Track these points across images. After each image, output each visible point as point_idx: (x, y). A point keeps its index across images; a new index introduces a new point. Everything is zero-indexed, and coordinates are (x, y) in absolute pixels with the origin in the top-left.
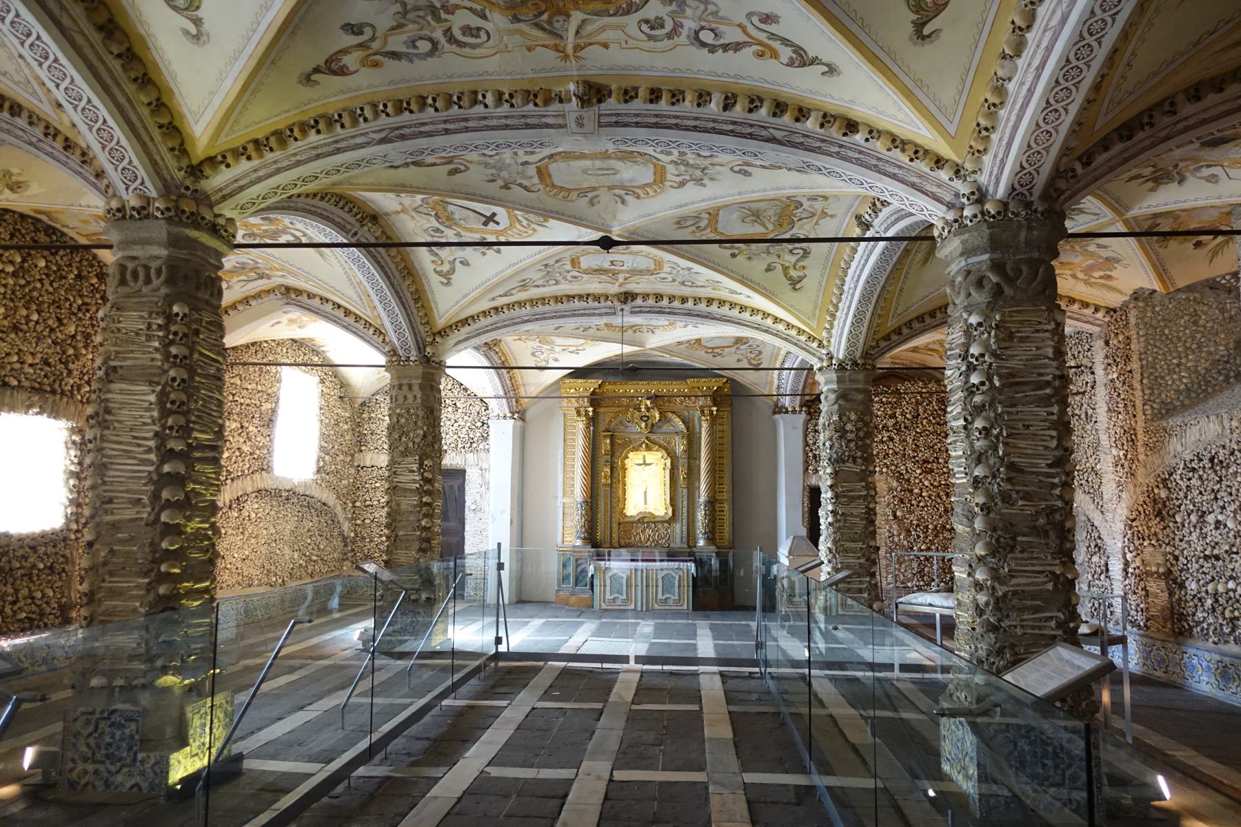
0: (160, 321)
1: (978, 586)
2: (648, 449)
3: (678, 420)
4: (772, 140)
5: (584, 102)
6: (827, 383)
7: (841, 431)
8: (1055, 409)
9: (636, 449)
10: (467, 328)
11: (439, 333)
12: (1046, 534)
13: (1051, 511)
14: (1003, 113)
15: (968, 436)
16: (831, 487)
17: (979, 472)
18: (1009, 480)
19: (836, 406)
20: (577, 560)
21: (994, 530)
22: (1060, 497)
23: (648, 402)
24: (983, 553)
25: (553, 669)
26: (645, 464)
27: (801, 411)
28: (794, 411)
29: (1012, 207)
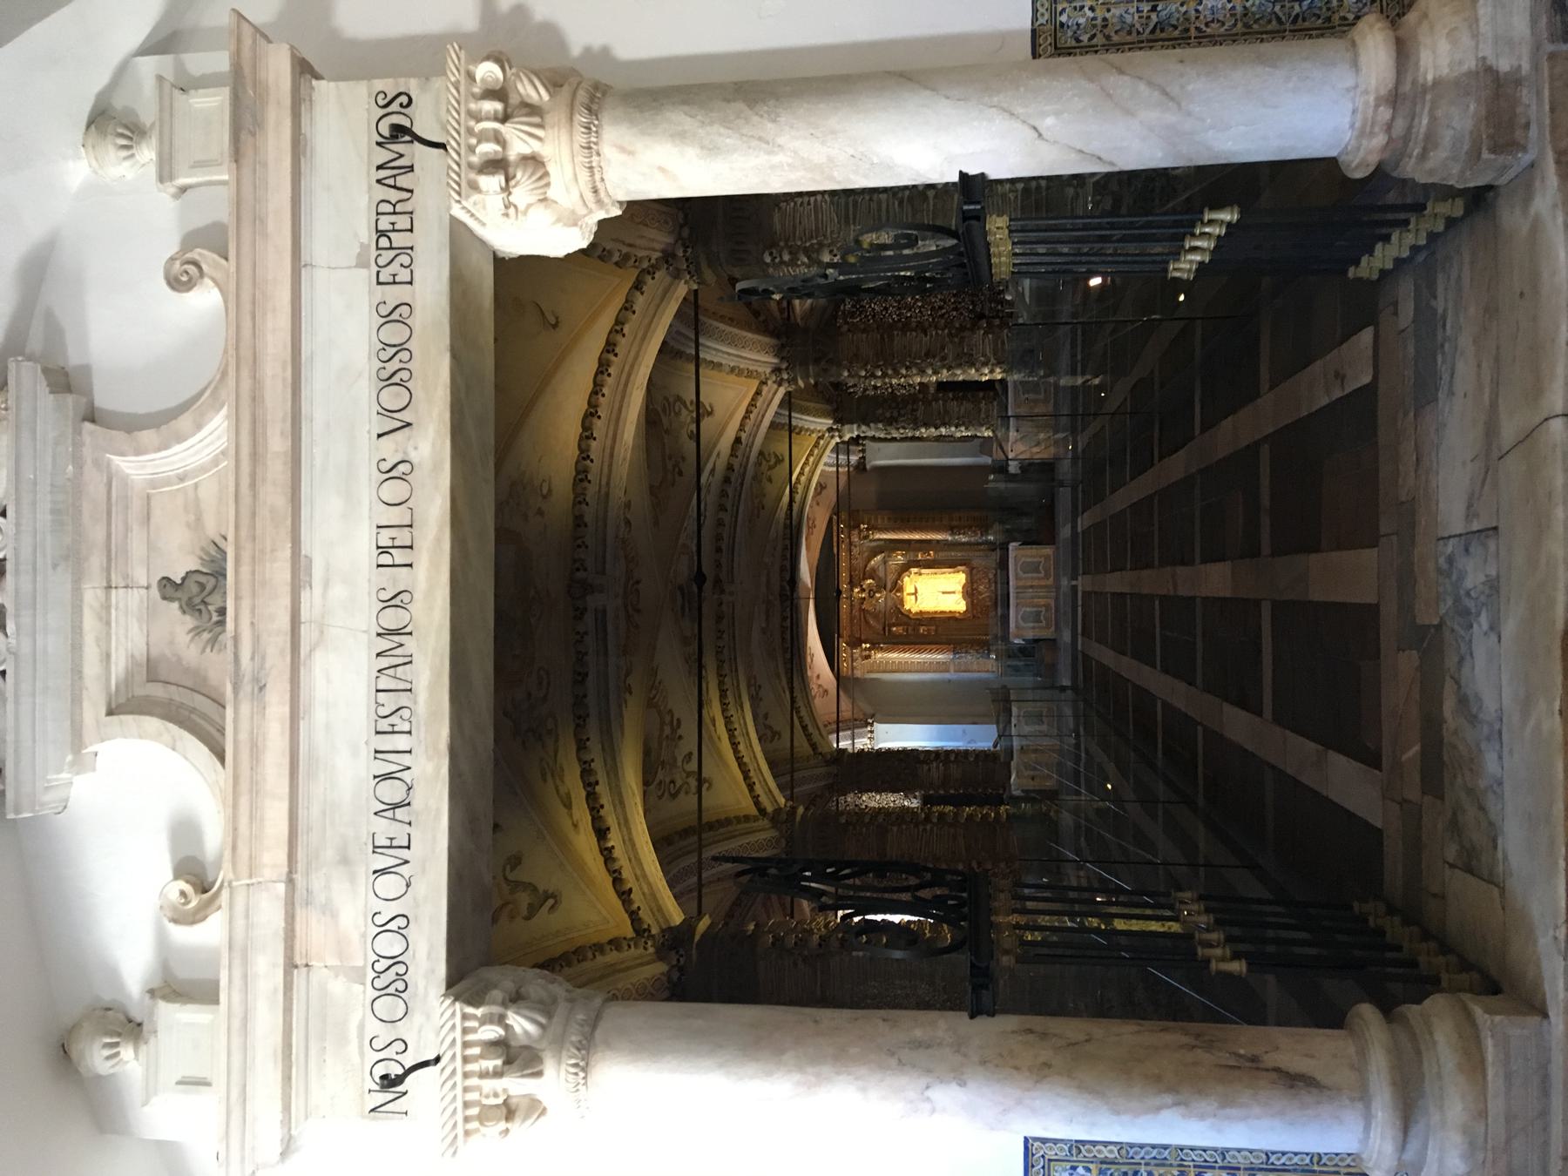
0: (851, 828)
1: (992, 372)
2: (901, 589)
3: (873, 562)
4: (742, 484)
5: (722, 592)
6: (853, 432)
7: (890, 422)
8: (896, 333)
9: (902, 601)
10: (811, 729)
11: (814, 750)
12: (963, 338)
13: (950, 334)
14: (742, 366)
15: (910, 376)
16: (936, 428)
17: (930, 372)
18: (934, 357)
19: (872, 425)
20: (1009, 657)
21: (961, 364)
22: (943, 330)
23: (856, 590)
24: (973, 371)
25: (1083, 645)
26: (915, 593)
27: (864, 445)
28: (863, 451)
29: (785, 354)
